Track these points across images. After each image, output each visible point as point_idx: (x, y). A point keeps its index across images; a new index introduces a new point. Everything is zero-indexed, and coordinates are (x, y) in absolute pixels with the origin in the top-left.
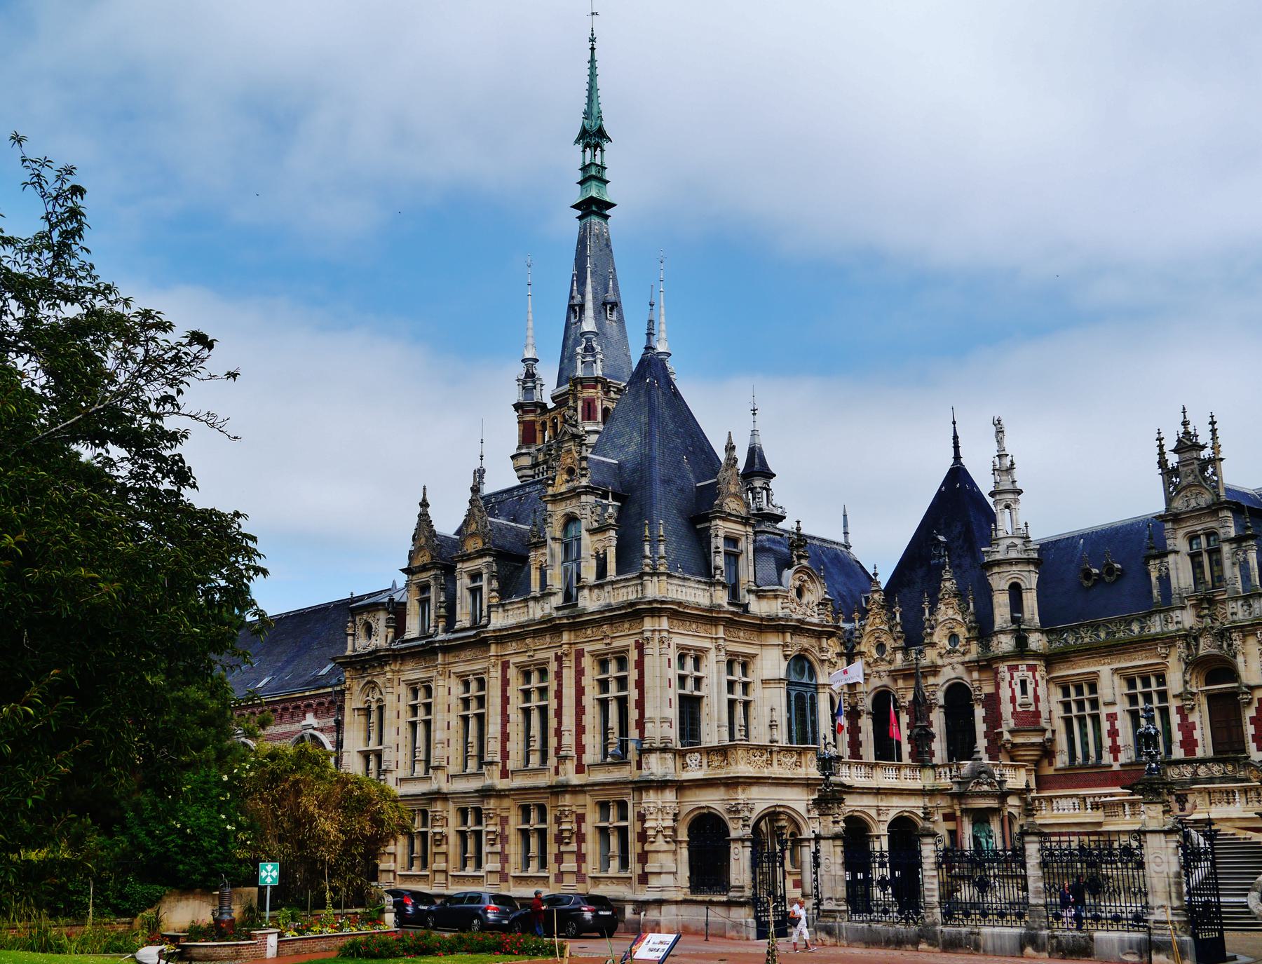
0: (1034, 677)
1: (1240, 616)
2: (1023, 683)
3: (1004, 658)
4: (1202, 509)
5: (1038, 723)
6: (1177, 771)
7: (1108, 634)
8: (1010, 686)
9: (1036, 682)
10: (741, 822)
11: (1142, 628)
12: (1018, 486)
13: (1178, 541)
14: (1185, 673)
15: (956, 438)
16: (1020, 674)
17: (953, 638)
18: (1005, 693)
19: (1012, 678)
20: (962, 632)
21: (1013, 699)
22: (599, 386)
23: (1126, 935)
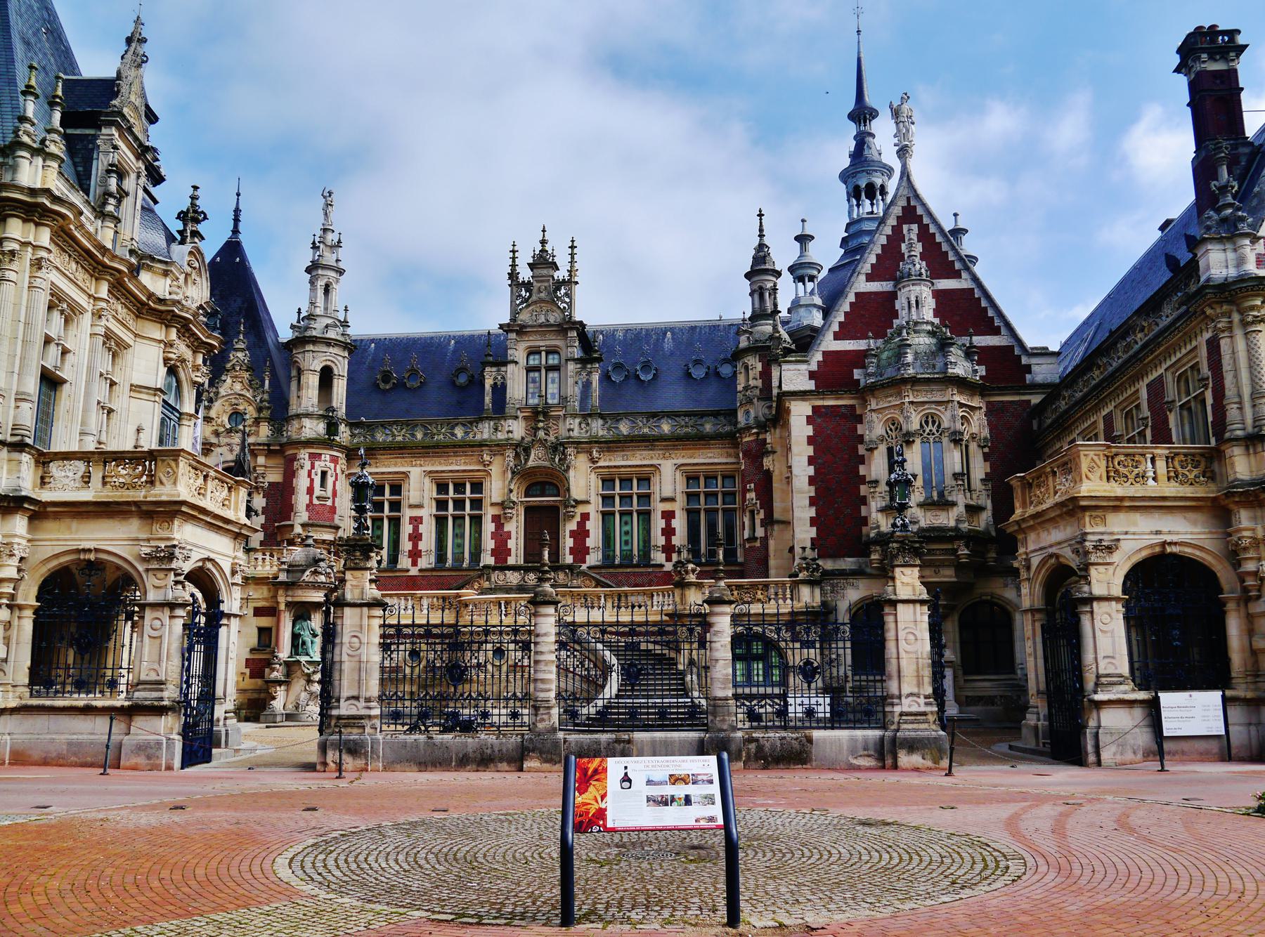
1: (575, 433)
2: (324, 474)
3: (309, 443)
4: (552, 325)
5: (333, 519)
6: (501, 577)
7: (425, 435)
8: (309, 475)
10: (172, 577)
11: (467, 433)
12: (341, 265)
13: (518, 352)
14: (511, 482)
15: (237, 211)
16: (322, 464)
17: (236, 416)
18: (302, 482)
19: (313, 467)
20: (251, 412)
21: (310, 491)
23: (859, 733)
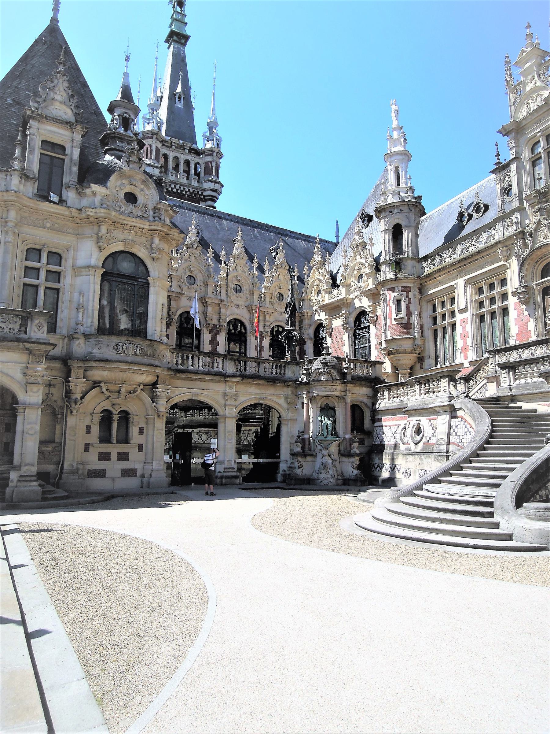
0: (408, 296)
2: (399, 302)
9: (410, 300)
22: (155, 136)
